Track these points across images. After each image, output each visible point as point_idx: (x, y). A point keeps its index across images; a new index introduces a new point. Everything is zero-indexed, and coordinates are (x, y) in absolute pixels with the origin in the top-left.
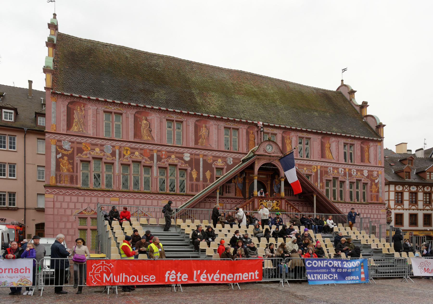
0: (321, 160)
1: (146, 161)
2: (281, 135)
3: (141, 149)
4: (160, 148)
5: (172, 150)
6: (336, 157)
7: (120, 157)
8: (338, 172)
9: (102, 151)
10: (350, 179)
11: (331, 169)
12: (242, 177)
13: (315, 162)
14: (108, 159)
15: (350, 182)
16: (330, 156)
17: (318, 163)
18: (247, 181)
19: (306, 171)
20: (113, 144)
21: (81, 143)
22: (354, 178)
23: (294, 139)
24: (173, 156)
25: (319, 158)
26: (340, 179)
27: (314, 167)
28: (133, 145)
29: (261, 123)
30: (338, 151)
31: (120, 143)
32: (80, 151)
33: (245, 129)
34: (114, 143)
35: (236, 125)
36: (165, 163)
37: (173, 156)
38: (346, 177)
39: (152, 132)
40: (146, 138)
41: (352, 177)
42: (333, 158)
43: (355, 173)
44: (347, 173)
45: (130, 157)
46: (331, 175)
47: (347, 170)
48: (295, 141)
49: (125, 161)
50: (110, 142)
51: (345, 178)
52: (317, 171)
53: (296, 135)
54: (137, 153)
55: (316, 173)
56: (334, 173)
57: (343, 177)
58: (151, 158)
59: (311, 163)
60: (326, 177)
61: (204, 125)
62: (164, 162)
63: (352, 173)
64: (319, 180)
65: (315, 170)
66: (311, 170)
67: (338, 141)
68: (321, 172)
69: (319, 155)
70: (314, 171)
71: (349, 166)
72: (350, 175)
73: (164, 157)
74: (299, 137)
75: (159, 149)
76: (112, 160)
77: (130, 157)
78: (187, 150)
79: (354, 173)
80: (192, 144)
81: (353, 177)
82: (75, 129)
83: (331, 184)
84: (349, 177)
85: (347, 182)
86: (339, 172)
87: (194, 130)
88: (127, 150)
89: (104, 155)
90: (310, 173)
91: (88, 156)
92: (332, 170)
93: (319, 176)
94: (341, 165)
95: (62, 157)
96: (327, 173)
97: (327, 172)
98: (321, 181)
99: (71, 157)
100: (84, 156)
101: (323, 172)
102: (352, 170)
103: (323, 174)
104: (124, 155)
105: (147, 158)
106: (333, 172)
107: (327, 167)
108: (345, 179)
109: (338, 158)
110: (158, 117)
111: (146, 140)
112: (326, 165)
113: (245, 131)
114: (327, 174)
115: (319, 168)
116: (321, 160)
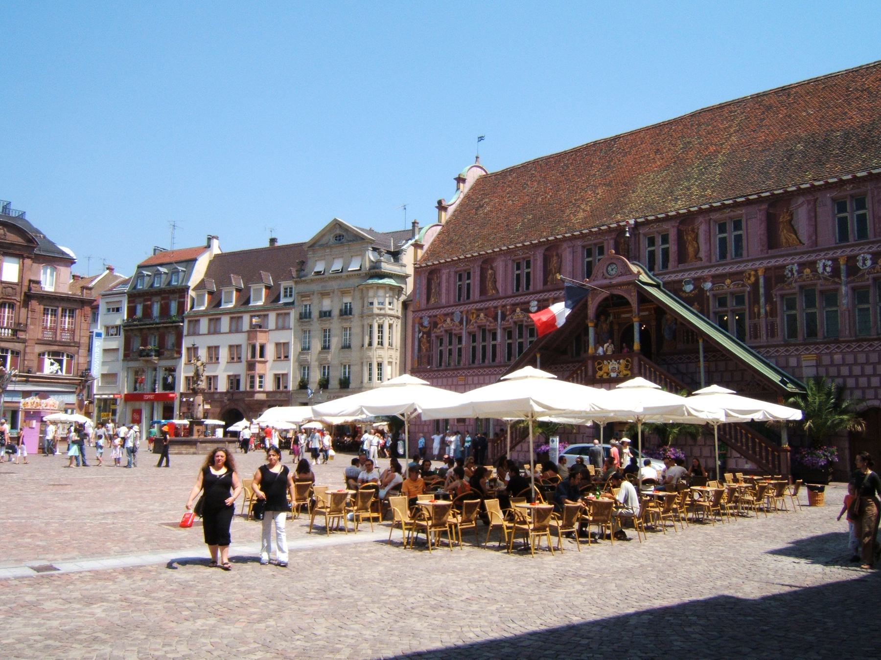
0: (767, 253)
1: (491, 322)
2: (676, 230)
3: (487, 309)
4: (504, 302)
5: (517, 301)
6: (810, 237)
7: (467, 324)
8: (815, 271)
9: (452, 320)
10: (853, 281)
11: (795, 268)
12: (608, 322)
13: (750, 264)
14: (458, 328)
15: (854, 289)
16: (791, 241)
17: (758, 263)
18: (616, 327)
19: (731, 286)
20: (462, 309)
21: (436, 316)
22: (867, 276)
23: (702, 229)
24: (518, 310)
25: (762, 251)
26: (819, 288)
27: (750, 275)
28: (479, 306)
29: (632, 222)
30: (816, 221)
31: (467, 306)
32: (435, 325)
33: (611, 239)
34: (462, 308)
35: (599, 237)
36: (510, 320)
37: (518, 310)
38: (839, 277)
39: (497, 283)
40: (491, 292)
41: (860, 273)
42: (800, 242)
43: (869, 263)
44: (843, 267)
45: (476, 322)
46: (796, 282)
47: (842, 262)
48: (706, 231)
49: (471, 328)
50: (459, 308)
51: (837, 280)
52: (757, 280)
53: (707, 218)
54: (482, 315)
55: (756, 285)
56: (801, 276)
57: (828, 280)
58: (496, 319)
59: (742, 267)
60: (782, 289)
61: (555, 254)
62: (508, 321)
63: (860, 264)
64: (762, 300)
65: (753, 279)
66: (743, 281)
67: (816, 200)
68: (767, 280)
69: (763, 246)
70: (749, 282)
71: (849, 250)
72: (853, 269)
73: (508, 313)
74: (715, 221)
75: (504, 303)
76: (461, 329)
77: (476, 322)
78: (533, 296)
79: (864, 263)
80: (540, 286)
81: (863, 275)
82: (432, 300)
83: (801, 302)
84: (848, 276)
85: (844, 289)
86: (816, 271)
87: (542, 264)
88: (473, 313)
89: (454, 325)
90: (740, 289)
91: (442, 329)
92: (797, 271)
93: (762, 291)
94: (823, 254)
95: (422, 337)
96: (782, 279)
97: (785, 276)
98: (769, 298)
99: (428, 334)
100: (439, 331)
101: (773, 279)
102: (860, 258)
103: (773, 282)
104: (471, 321)
105: (491, 319)
106: (798, 274)
107: (783, 267)
108: (837, 283)
109: (814, 238)
110: (503, 261)
111: (491, 296)
112: (781, 262)
113: (612, 242)
114: (784, 282)
115: (760, 273)
116: (767, 253)
